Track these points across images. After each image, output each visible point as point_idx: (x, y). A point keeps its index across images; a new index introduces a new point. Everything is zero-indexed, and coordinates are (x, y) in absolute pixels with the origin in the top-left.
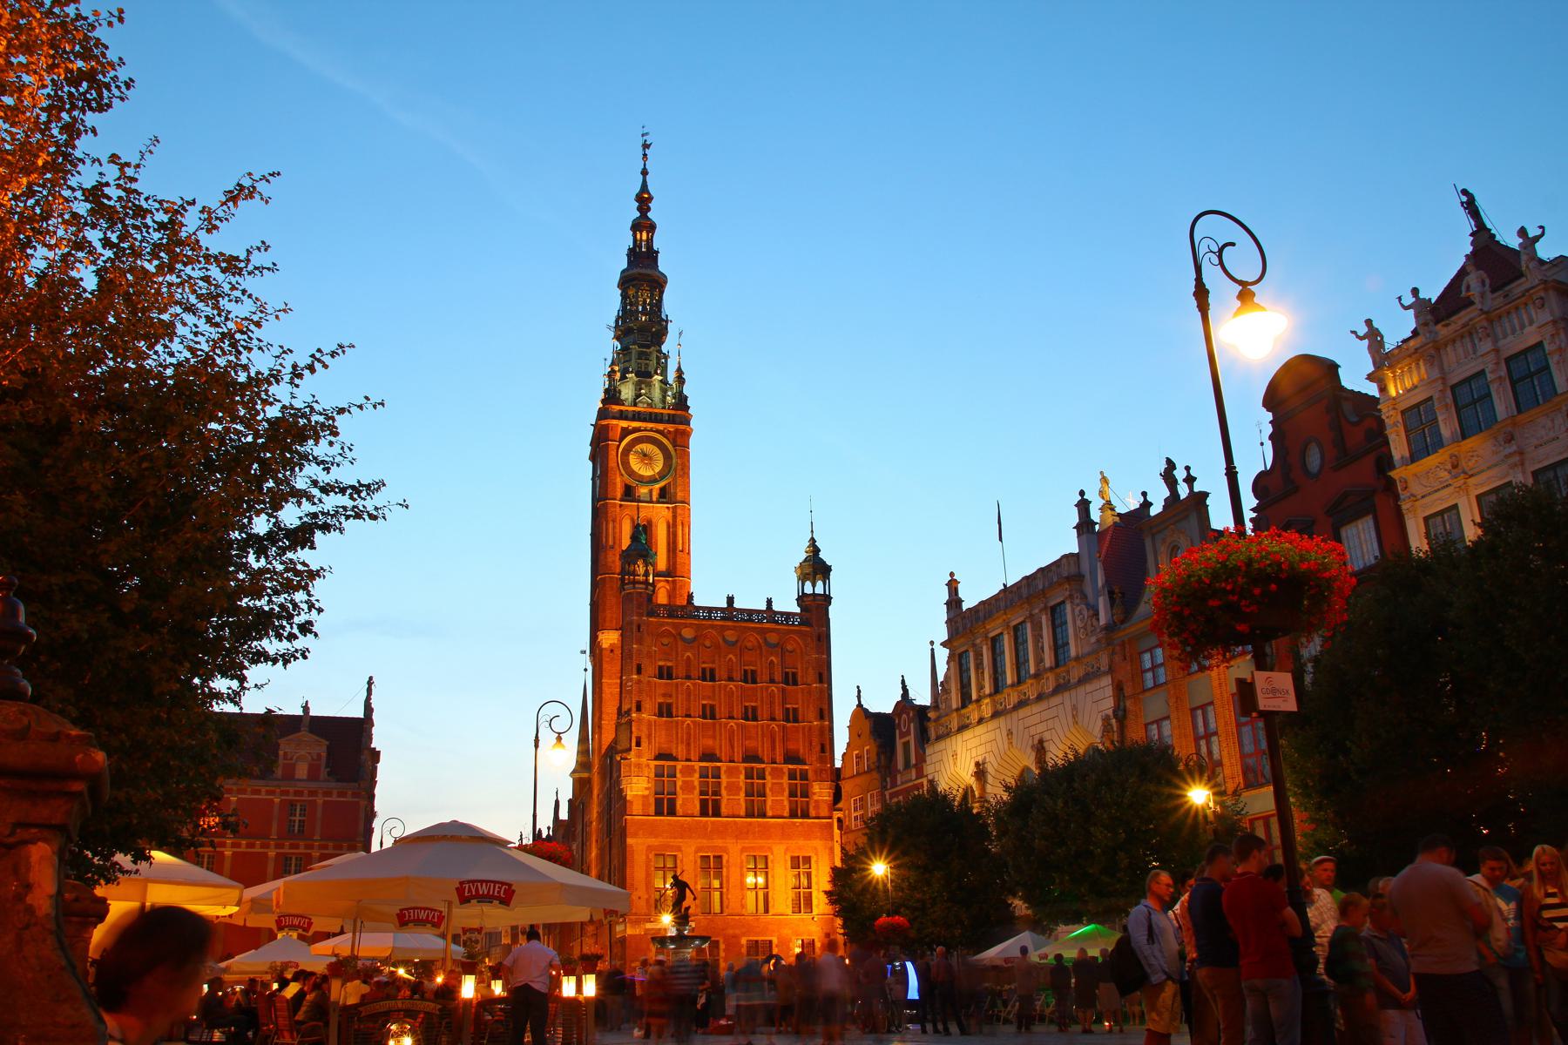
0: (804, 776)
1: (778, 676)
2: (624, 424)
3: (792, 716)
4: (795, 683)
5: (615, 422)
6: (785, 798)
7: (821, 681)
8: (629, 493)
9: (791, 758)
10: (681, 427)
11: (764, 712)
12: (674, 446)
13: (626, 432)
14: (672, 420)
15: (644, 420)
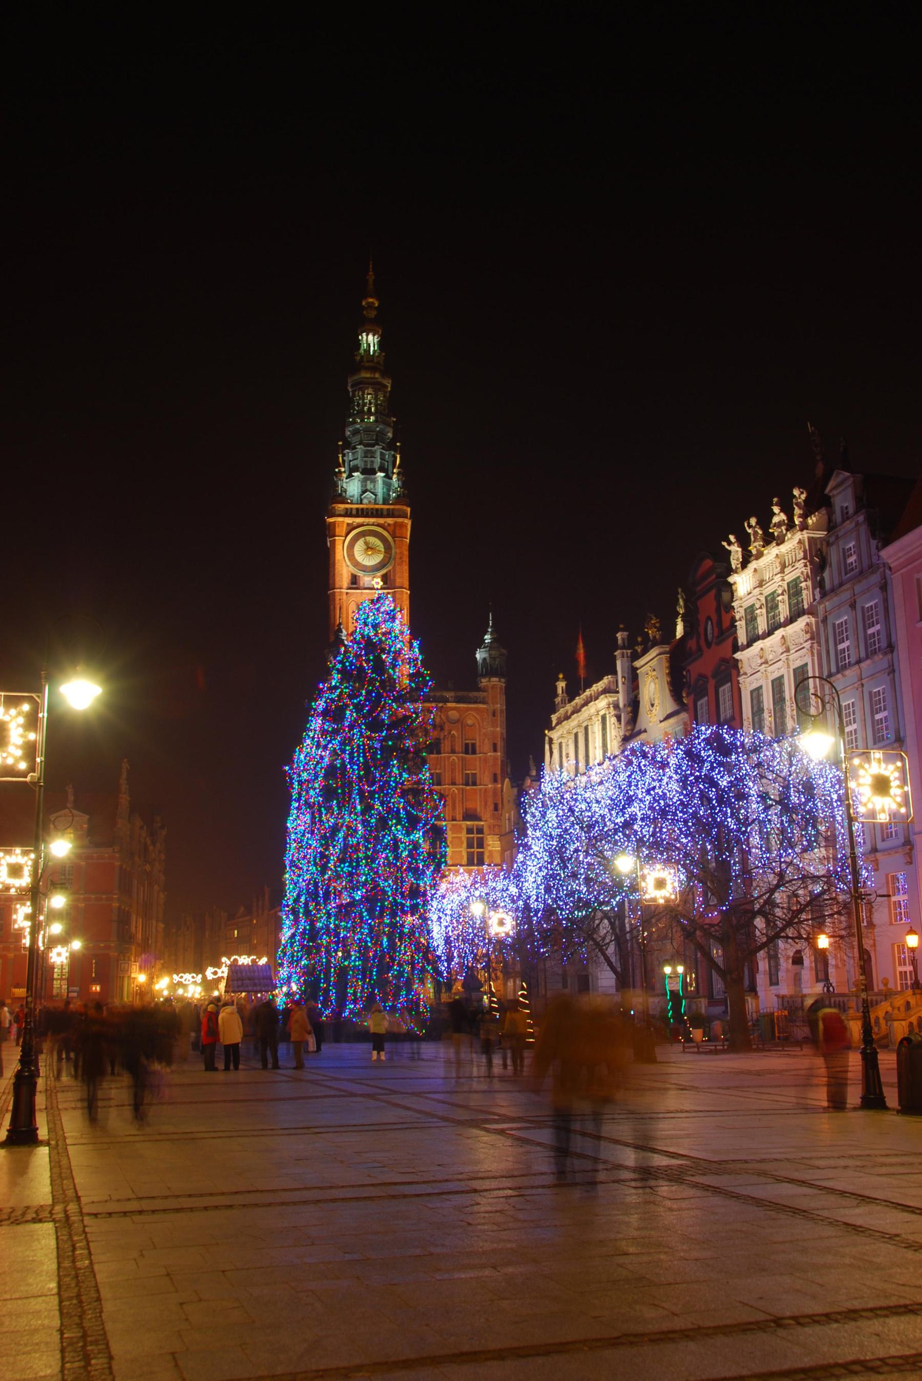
0: (480, 831)
1: (458, 748)
2: (349, 520)
3: (471, 781)
4: (474, 752)
5: (340, 519)
6: (464, 851)
7: (495, 750)
8: (354, 582)
9: (470, 815)
10: (400, 520)
11: (447, 777)
12: (394, 537)
13: (351, 528)
14: (390, 514)
15: (367, 516)
